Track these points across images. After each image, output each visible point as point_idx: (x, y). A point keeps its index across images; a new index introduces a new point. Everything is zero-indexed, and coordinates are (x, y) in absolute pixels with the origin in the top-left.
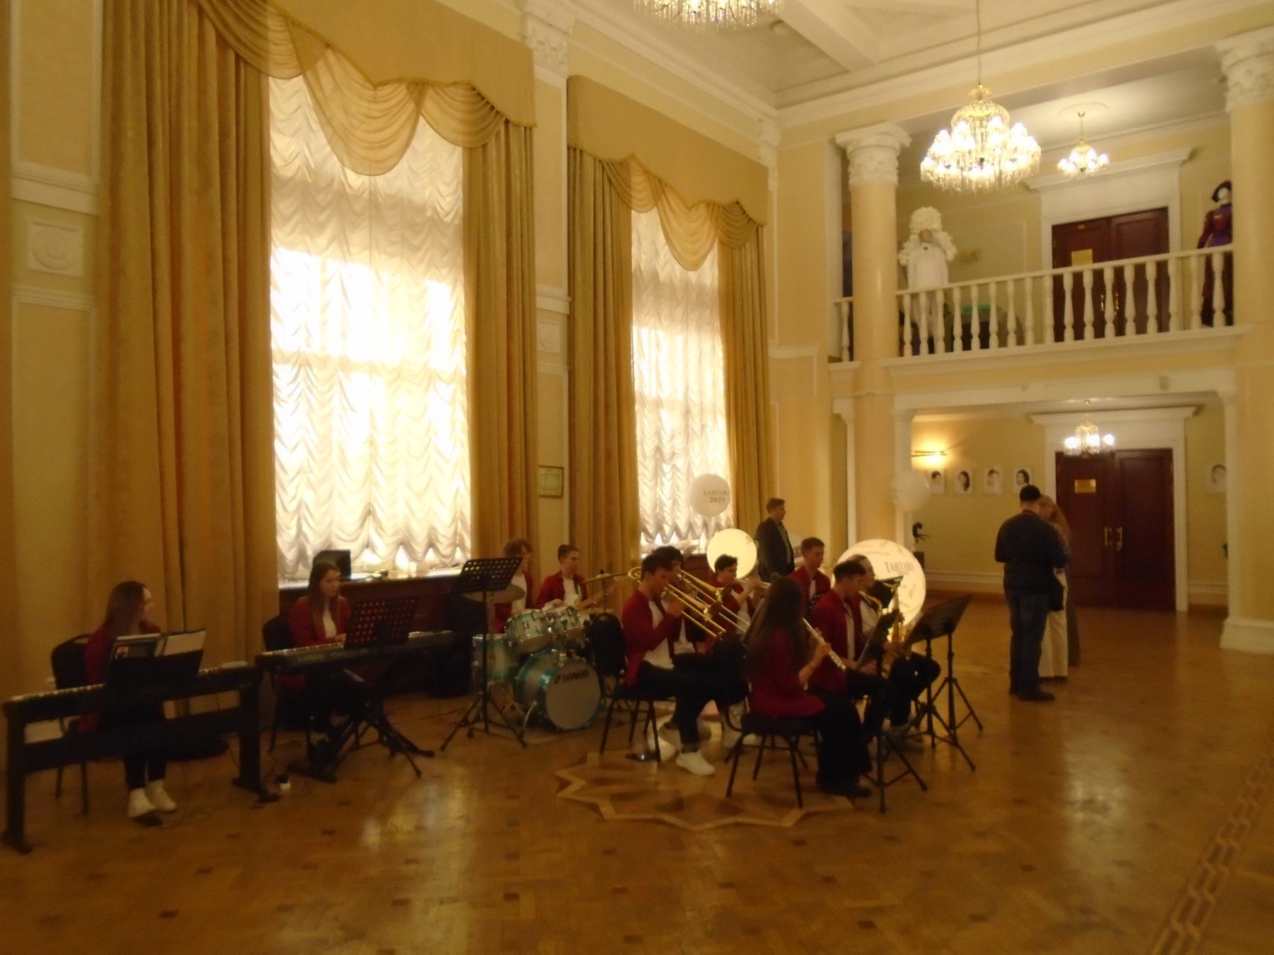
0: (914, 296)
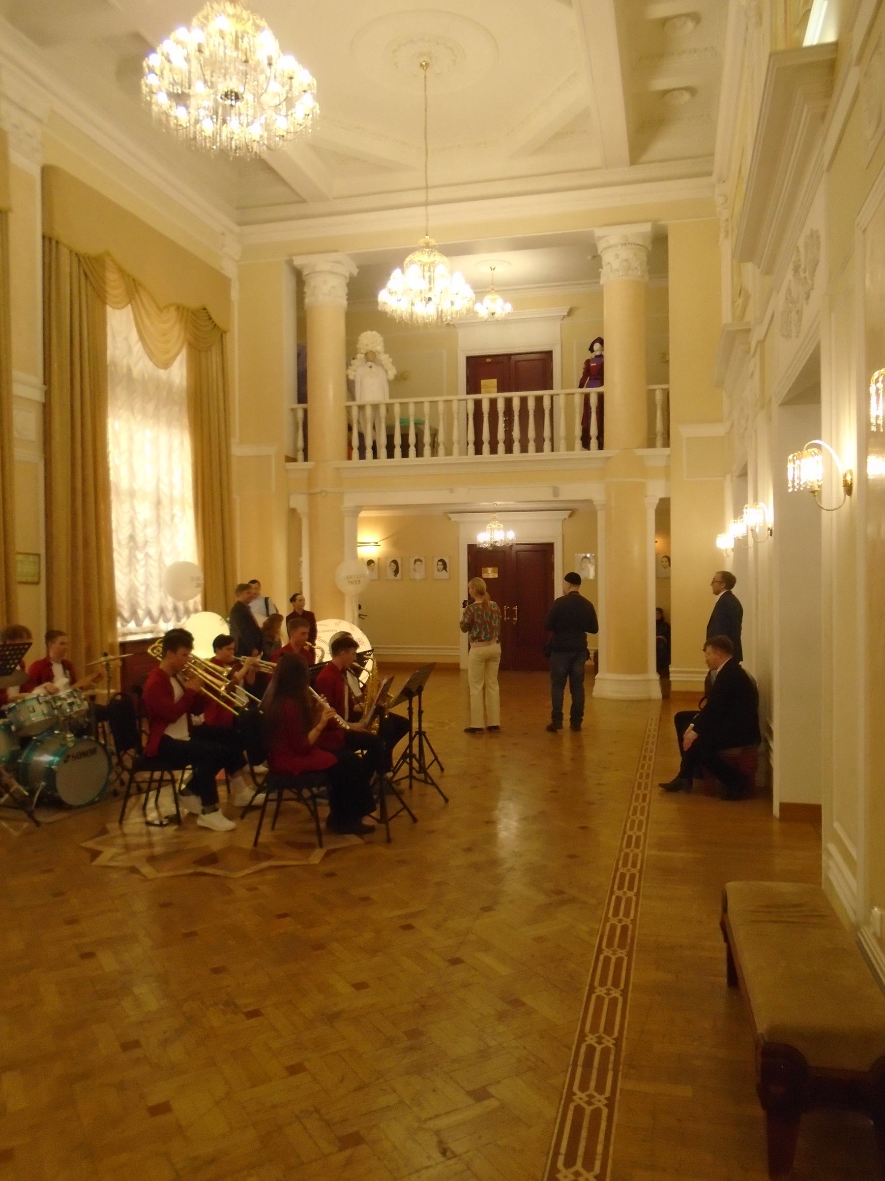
0: (361, 408)
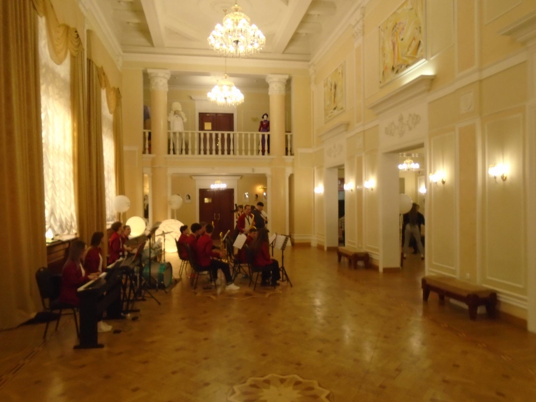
0: (175, 133)
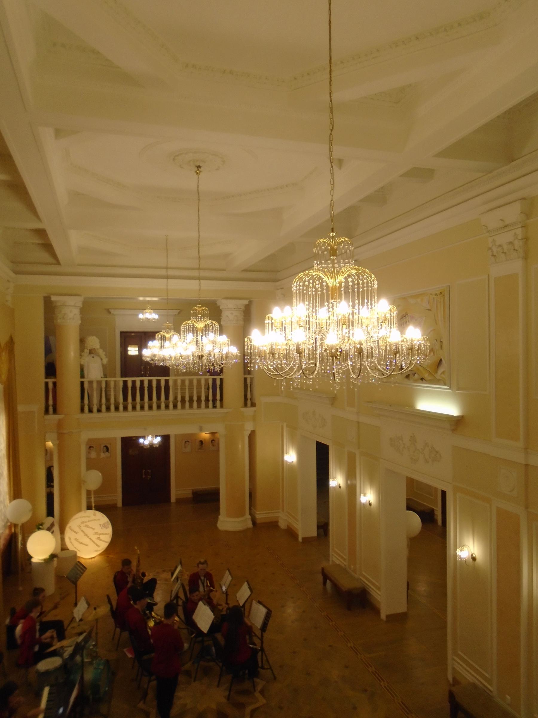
0: (91, 382)
